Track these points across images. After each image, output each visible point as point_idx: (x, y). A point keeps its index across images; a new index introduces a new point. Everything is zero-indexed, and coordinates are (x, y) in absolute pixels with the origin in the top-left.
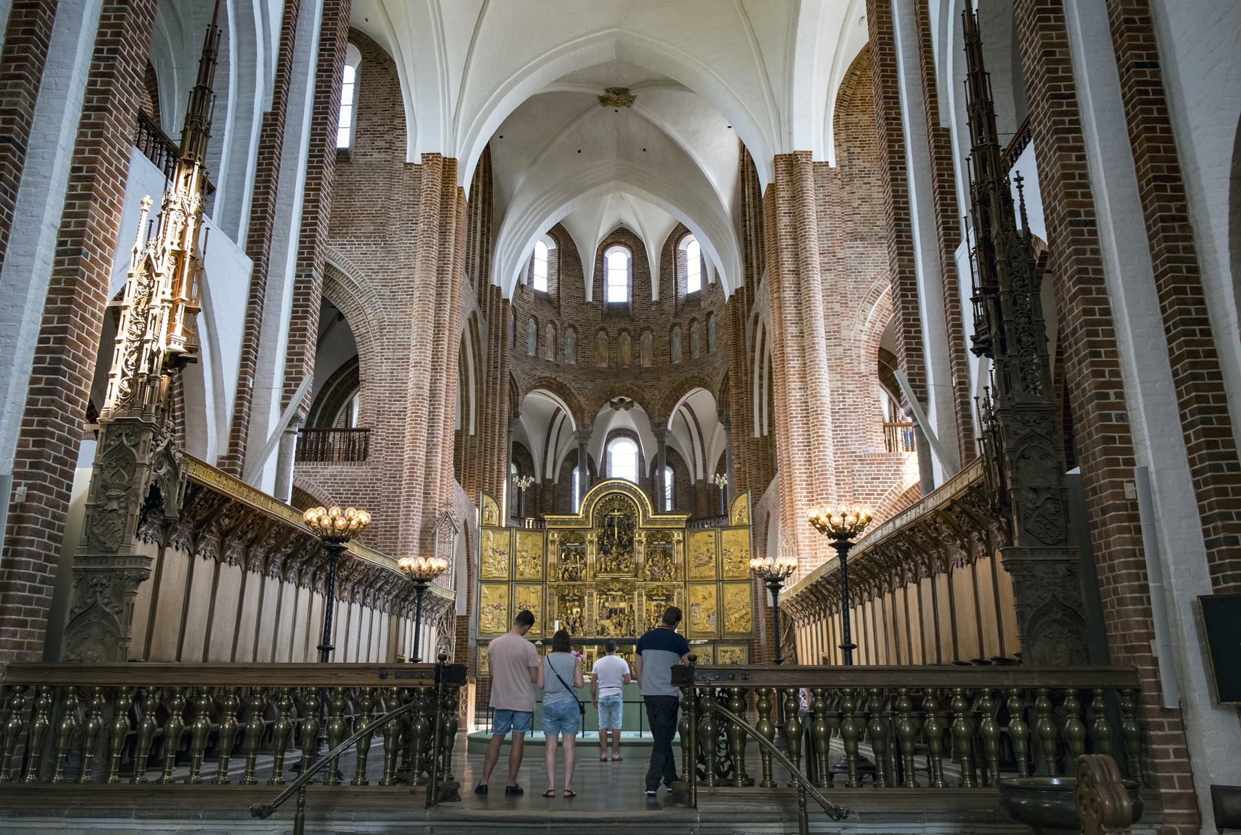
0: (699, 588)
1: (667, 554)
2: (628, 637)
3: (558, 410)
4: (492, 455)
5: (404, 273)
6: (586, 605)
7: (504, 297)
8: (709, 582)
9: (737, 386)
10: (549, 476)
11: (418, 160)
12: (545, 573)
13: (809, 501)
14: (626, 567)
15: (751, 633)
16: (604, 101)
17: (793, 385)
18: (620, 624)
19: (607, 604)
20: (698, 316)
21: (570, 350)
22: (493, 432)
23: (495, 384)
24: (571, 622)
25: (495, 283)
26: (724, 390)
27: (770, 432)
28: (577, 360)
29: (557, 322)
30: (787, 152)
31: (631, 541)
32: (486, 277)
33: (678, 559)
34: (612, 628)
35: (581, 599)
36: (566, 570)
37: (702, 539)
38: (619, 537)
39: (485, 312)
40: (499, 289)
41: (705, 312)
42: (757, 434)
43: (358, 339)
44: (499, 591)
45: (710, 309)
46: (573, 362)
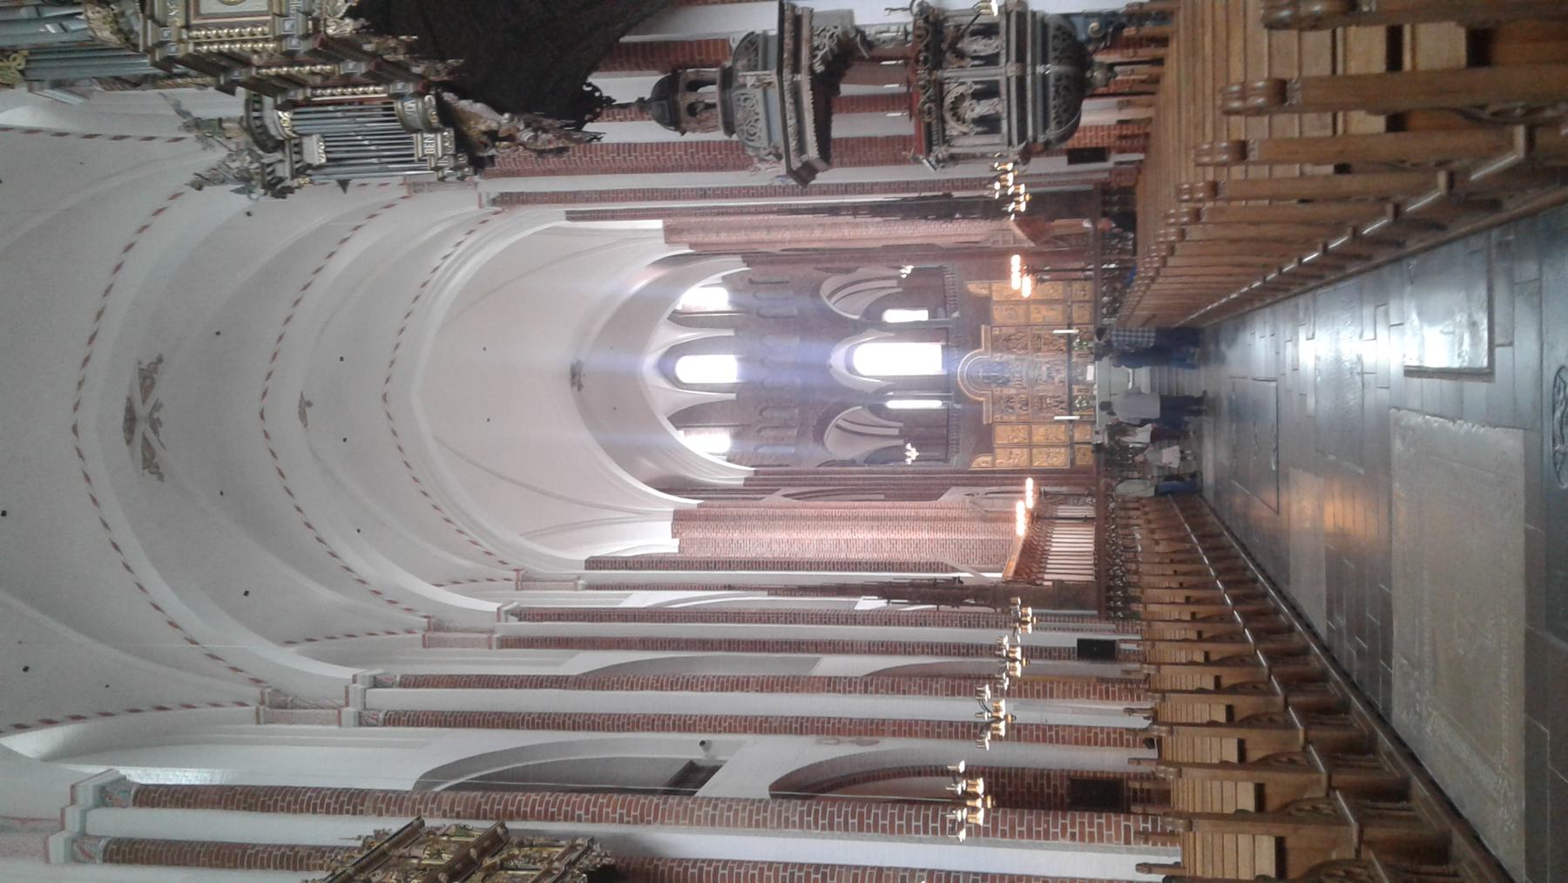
1: (1008, 339)
3: (838, 427)
4: (900, 479)
5: (775, 546)
7: (752, 475)
8: (1029, 309)
10: (896, 432)
11: (676, 542)
12: (1024, 423)
16: (580, 387)
17: (864, 233)
18: (1058, 370)
22: (880, 478)
25: (742, 482)
26: (827, 270)
28: (795, 407)
29: (759, 427)
30: (662, 234)
31: (1000, 363)
32: (733, 490)
33: (1012, 330)
34: (1060, 376)
35: (1041, 398)
37: (999, 314)
40: (746, 479)
46: (797, 411)
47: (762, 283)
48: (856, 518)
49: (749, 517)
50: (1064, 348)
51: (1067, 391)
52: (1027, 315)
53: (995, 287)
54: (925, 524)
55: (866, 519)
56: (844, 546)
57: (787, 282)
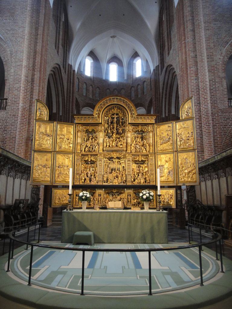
0: (162, 156)
2: (122, 184)
5: (21, 30)
6: (98, 166)
9: (155, 101)
13: (200, 127)
14: (121, 145)
15: (196, 182)
19: (110, 166)
20: (139, 83)
21: (98, 95)
23: (70, 98)
24: (89, 175)
27: (169, 115)
29: (93, 86)
31: (124, 131)
36: (86, 146)
37: (164, 129)
38: (117, 129)
39: (65, 72)
40: (71, 66)
41: (143, 81)
42: (164, 116)
43: (4, 63)
44: (46, 157)
45: (144, 80)
47: (143, 86)
48: (34, 70)
49: (38, 17)
50: (136, 183)
51: (100, 184)
52: (164, 152)
53: (189, 123)
54: (27, 106)
55: (33, 75)
56: (19, 64)
57: (144, 94)
